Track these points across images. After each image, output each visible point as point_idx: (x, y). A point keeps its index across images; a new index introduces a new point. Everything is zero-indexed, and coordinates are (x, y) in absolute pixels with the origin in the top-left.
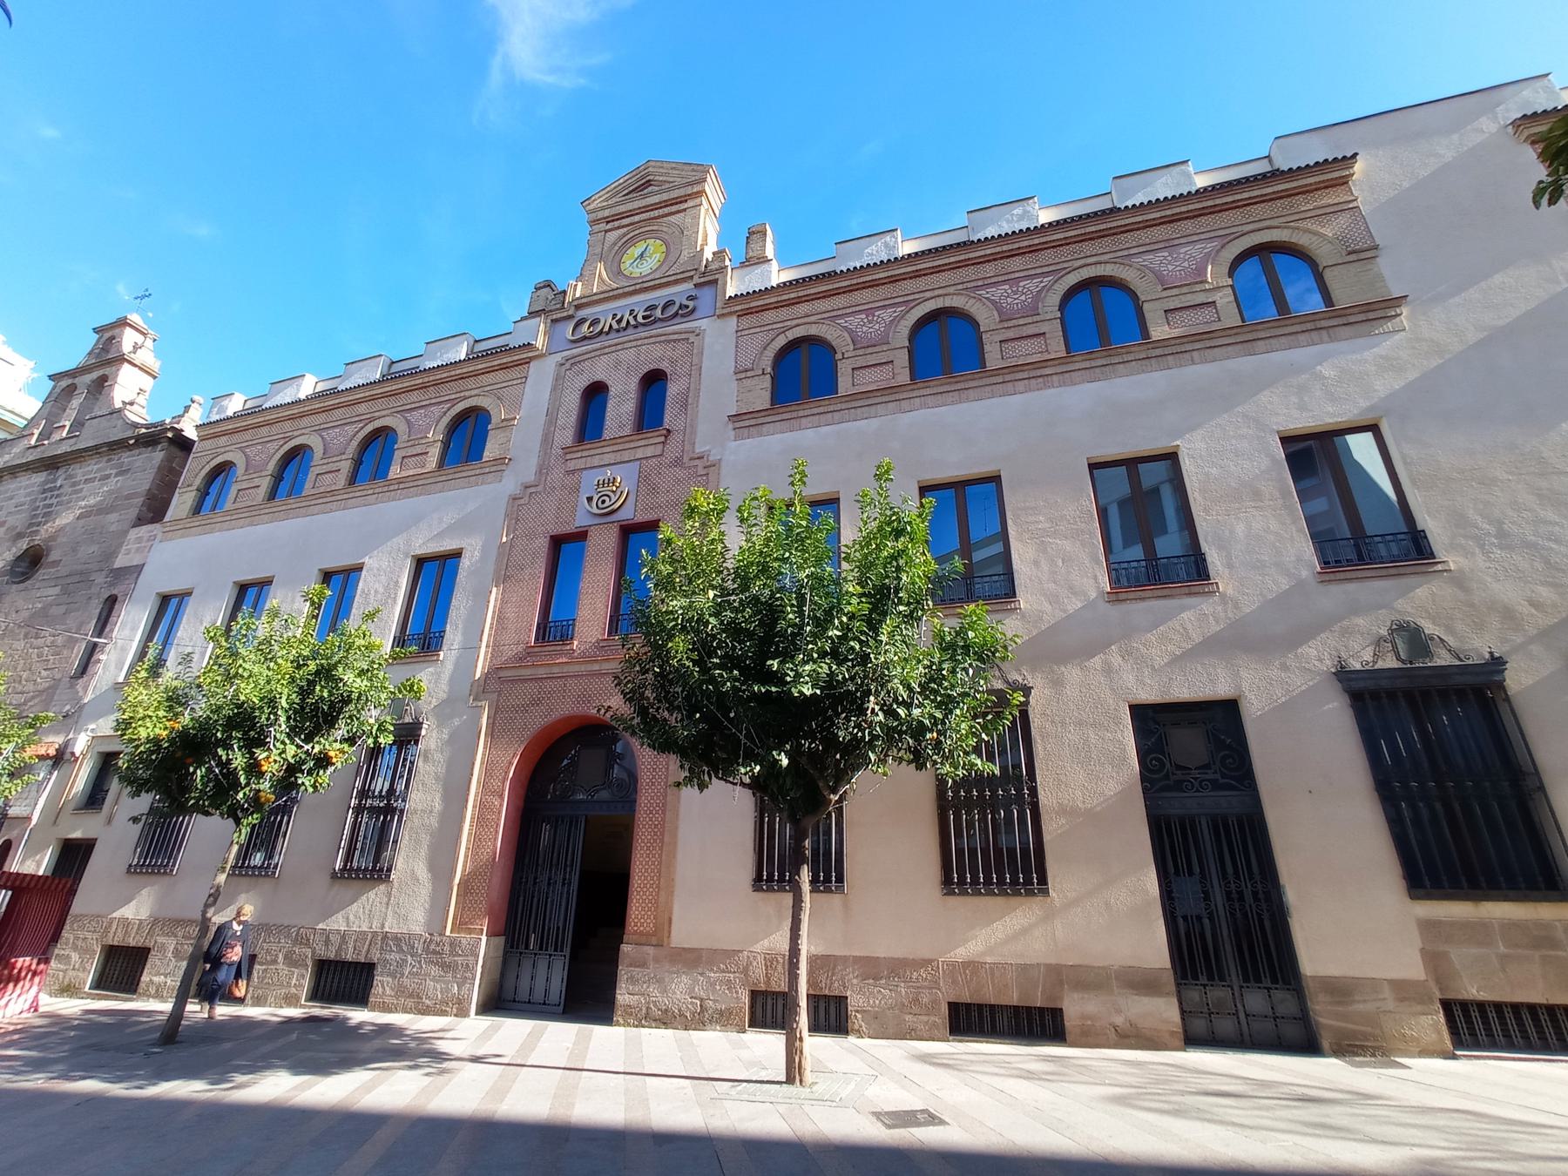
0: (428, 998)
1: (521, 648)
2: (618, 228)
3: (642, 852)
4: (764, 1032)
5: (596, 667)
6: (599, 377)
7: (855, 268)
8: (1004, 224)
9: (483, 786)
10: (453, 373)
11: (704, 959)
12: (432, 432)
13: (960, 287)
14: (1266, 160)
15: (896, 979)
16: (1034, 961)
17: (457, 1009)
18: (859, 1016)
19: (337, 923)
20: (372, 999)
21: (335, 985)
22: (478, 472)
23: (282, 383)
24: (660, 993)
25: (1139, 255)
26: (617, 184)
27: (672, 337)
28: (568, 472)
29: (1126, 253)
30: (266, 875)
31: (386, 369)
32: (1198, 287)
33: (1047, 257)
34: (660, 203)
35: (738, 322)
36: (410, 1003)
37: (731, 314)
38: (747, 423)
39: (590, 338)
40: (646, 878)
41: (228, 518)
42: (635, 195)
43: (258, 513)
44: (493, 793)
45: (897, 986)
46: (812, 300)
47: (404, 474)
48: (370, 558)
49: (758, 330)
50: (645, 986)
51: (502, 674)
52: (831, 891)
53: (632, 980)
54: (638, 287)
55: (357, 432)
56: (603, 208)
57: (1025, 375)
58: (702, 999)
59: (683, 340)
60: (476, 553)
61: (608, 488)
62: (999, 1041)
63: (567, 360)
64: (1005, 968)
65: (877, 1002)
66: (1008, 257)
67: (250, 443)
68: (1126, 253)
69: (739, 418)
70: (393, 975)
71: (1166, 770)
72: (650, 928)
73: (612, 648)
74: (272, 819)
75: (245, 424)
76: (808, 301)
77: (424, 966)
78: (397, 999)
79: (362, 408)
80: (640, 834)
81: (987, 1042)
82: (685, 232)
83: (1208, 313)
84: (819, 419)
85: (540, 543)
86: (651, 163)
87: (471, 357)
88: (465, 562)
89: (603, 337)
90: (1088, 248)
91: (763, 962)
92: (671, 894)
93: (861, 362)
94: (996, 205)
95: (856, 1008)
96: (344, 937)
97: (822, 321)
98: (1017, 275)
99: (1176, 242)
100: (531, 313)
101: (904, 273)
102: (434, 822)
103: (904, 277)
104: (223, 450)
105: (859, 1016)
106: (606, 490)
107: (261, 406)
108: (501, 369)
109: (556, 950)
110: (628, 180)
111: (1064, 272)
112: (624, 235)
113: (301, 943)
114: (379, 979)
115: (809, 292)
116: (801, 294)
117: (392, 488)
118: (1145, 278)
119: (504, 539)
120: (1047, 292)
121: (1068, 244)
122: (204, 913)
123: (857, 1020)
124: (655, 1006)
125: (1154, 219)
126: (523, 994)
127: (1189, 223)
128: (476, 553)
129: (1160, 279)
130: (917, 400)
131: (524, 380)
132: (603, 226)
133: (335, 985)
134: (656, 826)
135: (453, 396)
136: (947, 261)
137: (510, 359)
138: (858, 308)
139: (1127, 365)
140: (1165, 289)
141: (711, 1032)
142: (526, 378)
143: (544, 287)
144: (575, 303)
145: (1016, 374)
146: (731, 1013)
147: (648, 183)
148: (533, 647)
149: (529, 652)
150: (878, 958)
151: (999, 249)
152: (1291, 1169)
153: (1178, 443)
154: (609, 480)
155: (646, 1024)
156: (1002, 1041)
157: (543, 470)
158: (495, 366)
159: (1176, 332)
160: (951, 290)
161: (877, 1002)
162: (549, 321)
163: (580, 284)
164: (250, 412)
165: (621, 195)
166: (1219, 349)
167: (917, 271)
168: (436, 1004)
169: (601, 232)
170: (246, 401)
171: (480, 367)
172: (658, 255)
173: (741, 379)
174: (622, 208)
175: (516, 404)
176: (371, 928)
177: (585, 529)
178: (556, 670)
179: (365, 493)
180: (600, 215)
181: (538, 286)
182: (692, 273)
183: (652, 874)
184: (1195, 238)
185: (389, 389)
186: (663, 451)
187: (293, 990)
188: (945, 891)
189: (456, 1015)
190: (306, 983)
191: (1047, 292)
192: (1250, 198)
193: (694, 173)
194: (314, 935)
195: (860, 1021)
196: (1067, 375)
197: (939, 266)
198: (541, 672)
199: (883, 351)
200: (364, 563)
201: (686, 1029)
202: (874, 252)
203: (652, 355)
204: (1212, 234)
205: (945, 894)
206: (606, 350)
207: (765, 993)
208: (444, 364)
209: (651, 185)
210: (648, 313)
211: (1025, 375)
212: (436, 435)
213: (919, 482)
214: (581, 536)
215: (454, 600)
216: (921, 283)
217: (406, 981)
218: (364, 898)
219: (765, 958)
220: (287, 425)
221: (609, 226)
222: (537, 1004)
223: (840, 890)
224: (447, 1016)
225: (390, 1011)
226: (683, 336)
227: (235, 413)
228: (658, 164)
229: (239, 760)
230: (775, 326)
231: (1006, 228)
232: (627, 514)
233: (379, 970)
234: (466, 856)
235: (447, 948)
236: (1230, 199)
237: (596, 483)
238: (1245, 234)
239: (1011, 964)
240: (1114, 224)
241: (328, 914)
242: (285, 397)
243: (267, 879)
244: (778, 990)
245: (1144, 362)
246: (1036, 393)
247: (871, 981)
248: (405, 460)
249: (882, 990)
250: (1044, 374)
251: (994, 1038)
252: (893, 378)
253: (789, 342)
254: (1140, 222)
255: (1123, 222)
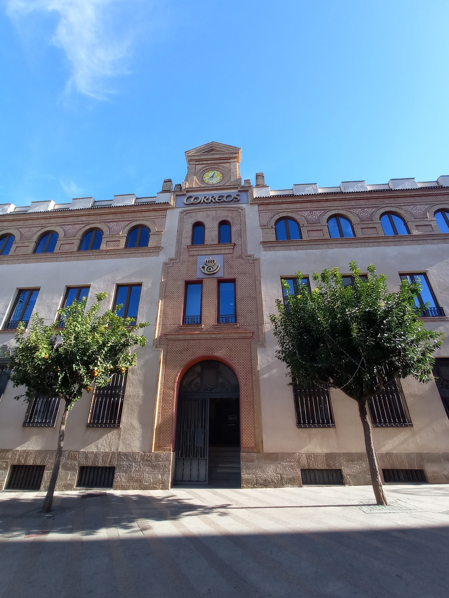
0: (145, 481)
1: (176, 326)
2: (201, 164)
3: (245, 413)
4: (310, 486)
5: (214, 336)
6: (200, 219)
7: (302, 195)
8: (356, 188)
9: (164, 385)
10: (130, 209)
11: (279, 457)
12: (121, 233)
13: (343, 207)
14: (436, 182)
15: (361, 461)
16: (411, 452)
17: (162, 486)
18: (348, 477)
19: (92, 448)
20: (115, 484)
21: (91, 478)
22: (147, 251)
23: (38, 203)
24: (261, 473)
25: (404, 206)
26: (200, 148)
27: (231, 209)
28: (191, 256)
29: (399, 204)
30: (49, 426)
31: (93, 203)
32: (425, 219)
33: (372, 202)
34: (219, 158)
35: (258, 207)
36: (136, 484)
37: (255, 204)
38: (269, 245)
39: (194, 204)
40: (248, 424)
41: (12, 259)
42: (207, 153)
43: (29, 258)
44: (169, 388)
45: (361, 464)
46: (288, 203)
47: (108, 248)
48: (93, 283)
49: (267, 211)
50: (254, 470)
51: (169, 337)
52: (330, 427)
53: (248, 468)
54: (214, 188)
55: (82, 228)
56: (195, 156)
57: (372, 241)
58: (281, 474)
59: (236, 210)
60: (149, 285)
61: (211, 264)
62: (404, 484)
63: (184, 211)
64: (401, 455)
65: (355, 471)
66: (359, 200)
67: (22, 227)
68: (399, 204)
69: (265, 243)
70: (125, 472)
71: (441, 381)
72: (253, 445)
73: (220, 328)
74: (50, 399)
75: (19, 218)
76: (286, 204)
77: (142, 467)
78: (129, 483)
79: (83, 218)
80: (243, 405)
81: (400, 484)
82: (231, 171)
83: (429, 228)
84: (198, 252)
85: (181, 283)
86: (213, 143)
87: (135, 204)
88: (144, 288)
89: (200, 205)
90: (386, 201)
91: (305, 457)
92: (261, 430)
93: (310, 229)
94: (352, 182)
95: (346, 474)
96: (96, 455)
97: (293, 212)
98: (363, 206)
99: (415, 204)
100: (163, 191)
101: (323, 199)
102: (140, 401)
103: (322, 201)
104: (6, 228)
105: (348, 477)
106: (210, 264)
107: (27, 211)
108: (153, 211)
109: (194, 457)
110: (204, 147)
111: (328, 210)
112: (204, 167)
113: (71, 459)
114: (117, 474)
115: (287, 200)
116: (284, 201)
117: (103, 254)
118: (407, 214)
119: (163, 280)
120: (375, 213)
121: (379, 198)
122: (59, 445)
123: (348, 478)
124: (260, 478)
125: (407, 195)
126: (186, 477)
127: (418, 198)
128: (149, 285)
129: (412, 215)
130: (334, 245)
131: (165, 217)
132: (194, 162)
133: (91, 478)
134: (250, 402)
135: (131, 219)
136: (338, 197)
137: (158, 207)
138: (306, 209)
139: (406, 242)
140: (415, 218)
141: (287, 488)
142: (166, 216)
143: (168, 181)
144: (187, 190)
145: (369, 240)
146: (294, 479)
147: (213, 150)
148: (181, 326)
149: (180, 328)
150: (352, 453)
151: (356, 196)
152: (390, 528)
153: (428, 270)
154: (211, 261)
155: (257, 486)
156: (406, 484)
157: (178, 253)
158: (150, 209)
159: (420, 233)
160: (341, 208)
161: (355, 471)
162: (175, 195)
163: (187, 183)
164: (19, 213)
165: (202, 152)
166: (435, 240)
167: (327, 199)
168: (150, 484)
169: (194, 164)
170: (15, 208)
171: (143, 209)
172: (219, 177)
173: (263, 229)
174: (203, 157)
175: (163, 225)
176: (111, 450)
177: (202, 279)
178: (195, 336)
179: (89, 254)
180: (193, 158)
181: (166, 181)
182: (237, 186)
183: (251, 422)
184: (421, 203)
185: (98, 212)
186: (233, 252)
187: (69, 482)
188: (375, 426)
189: (161, 489)
190: (76, 478)
191: (375, 213)
192: (437, 193)
193: (233, 150)
194: (79, 454)
195: (349, 479)
196: (386, 243)
197: (335, 199)
198: (188, 337)
199: (318, 226)
200: (91, 285)
201: (275, 488)
202: (309, 190)
203: (224, 215)
204: (427, 203)
205: (375, 427)
206: (202, 210)
207: (309, 470)
208: (125, 205)
209: (213, 151)
210: (220, 198)
211: (372, 241)
212: (123, 234)
213: (280, 276)
214: (200, 282)
215: (140, 304)
216: (329, 204)
217: (133, 475)
218: (105, 436)
219: (306, 455)
220: (43, 221)
221: (197, 163)
222: (187, 481)
223: (334, 426)
224: (157, 489)
225: (126, 489)
226: (237, 209)
227: (11, 212)
228: (217, 144)
229: (82, 370)
230: (274, 211)
231: (356, 190)
232: (221, 275)
233: (118, 470)
234: (159, 416)
235: (153, 458)
236: (431, 193)
237: (205, 261)
238: (437, 204)
239: (403, 453)
240: (395, 194)
241: (86, 443)
242: (41, 208)
243: (48, 429)
244: (313, 468)
245: (412, 241)
246: (377, 247)
247: (351, 462)
248: (108, 243)
249: (356, 466)
250: (379, 241)
251: (404, 483)
252: (323, 236)
253: (281, 217)
254: (403, 195)
255: (397, 194)
